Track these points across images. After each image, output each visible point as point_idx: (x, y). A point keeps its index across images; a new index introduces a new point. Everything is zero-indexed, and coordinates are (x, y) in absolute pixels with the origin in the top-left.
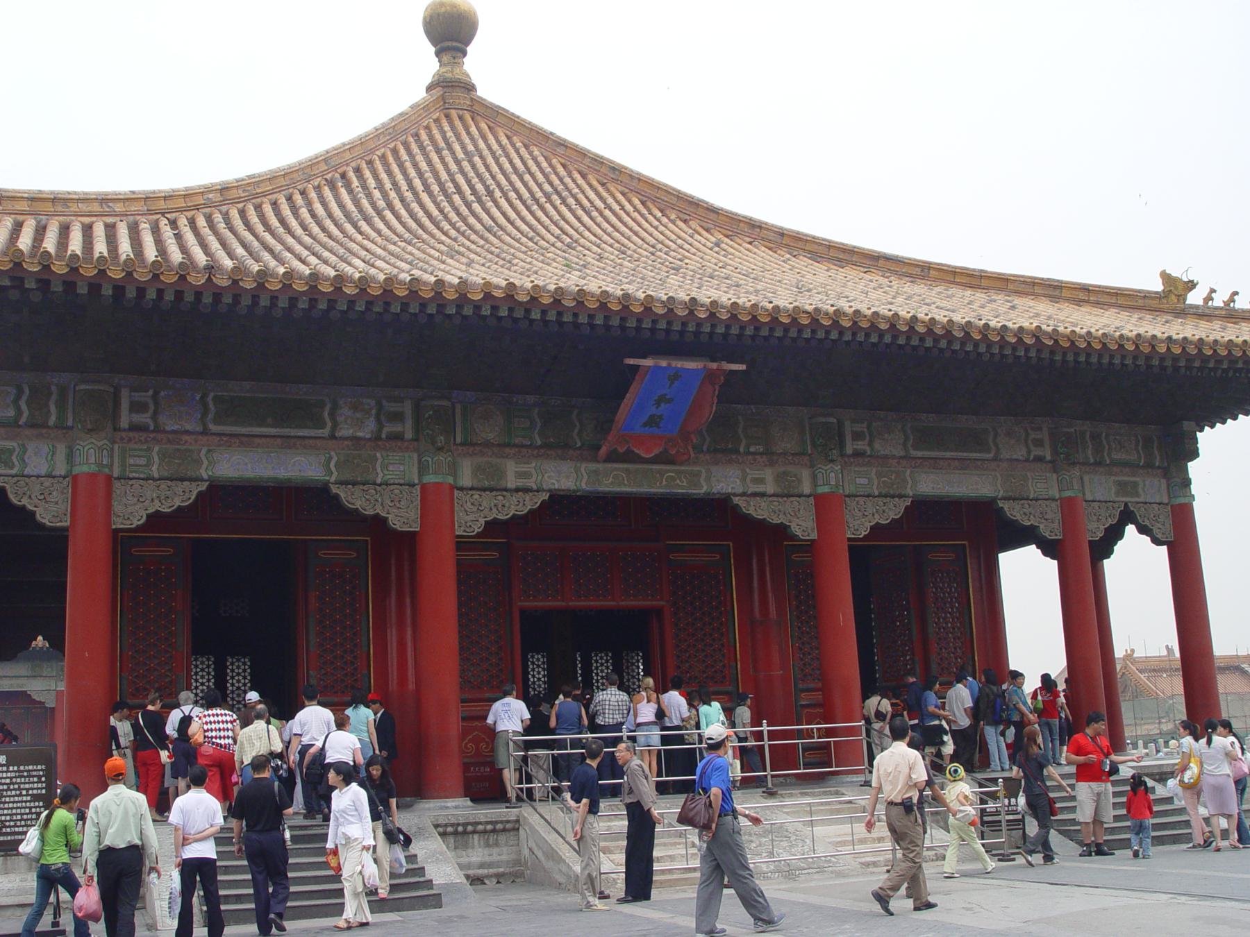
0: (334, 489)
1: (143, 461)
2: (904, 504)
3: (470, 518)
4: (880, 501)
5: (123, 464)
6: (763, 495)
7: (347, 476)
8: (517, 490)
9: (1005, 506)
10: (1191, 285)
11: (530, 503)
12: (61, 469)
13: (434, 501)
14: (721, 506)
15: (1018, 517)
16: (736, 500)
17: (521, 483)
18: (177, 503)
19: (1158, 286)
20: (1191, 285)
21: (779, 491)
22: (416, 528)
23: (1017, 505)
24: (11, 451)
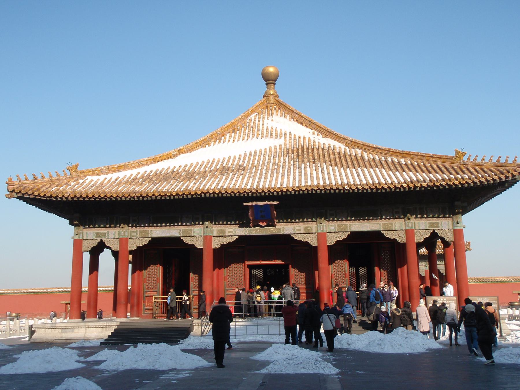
0: (182, 238)
1: (135, 234)
2: (347, 234)
3: (217, 244)
4: (339, 234)
5: (131, 235)
6: (300, 234)
7: (185, 235)
8: (229, 236)
9: (384, 233)
10: (464, 154)
11: (233, 239)
12: (117, 237)
13: (208, 239)
14: (288, 237)
15: (389, 236)
16: (292, 236)
17: (229, 234)
18: (144, 244)
19: (453, 154)
20: (464, 154)
21: (305, 232)
22: (316, 245)
23: (389, 233)
24: (106, 233)
